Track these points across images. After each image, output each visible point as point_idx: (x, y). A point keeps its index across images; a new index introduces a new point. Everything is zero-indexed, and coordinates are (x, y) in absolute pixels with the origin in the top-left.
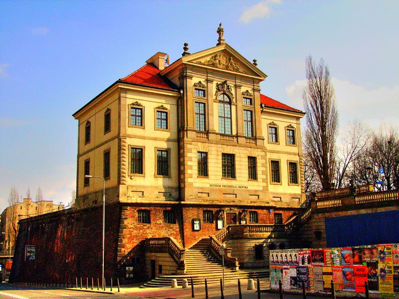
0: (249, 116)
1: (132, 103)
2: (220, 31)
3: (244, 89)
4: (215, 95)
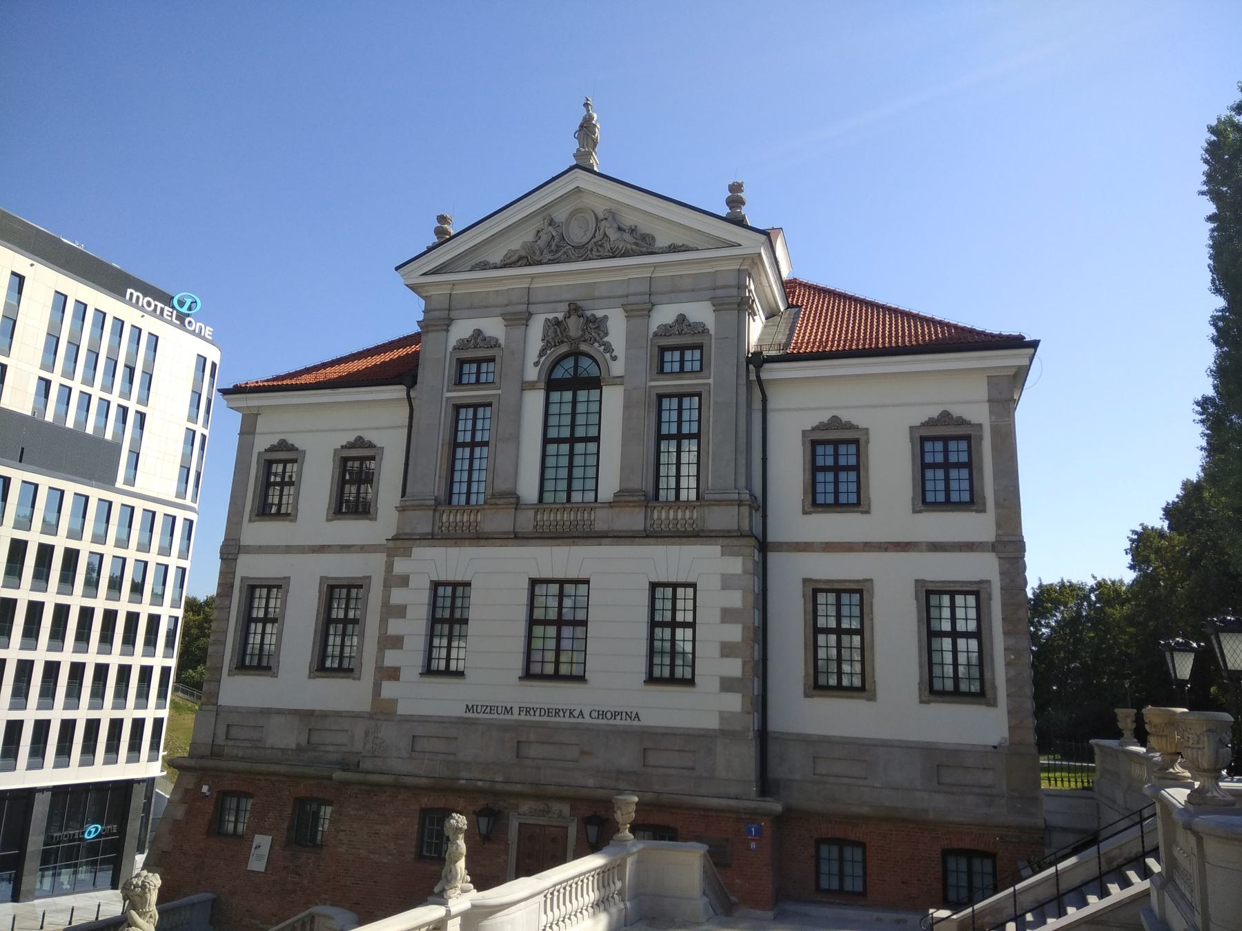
1: (268, 446)
2: (586, 129)
3: (664, 315)
4: (536, 364)
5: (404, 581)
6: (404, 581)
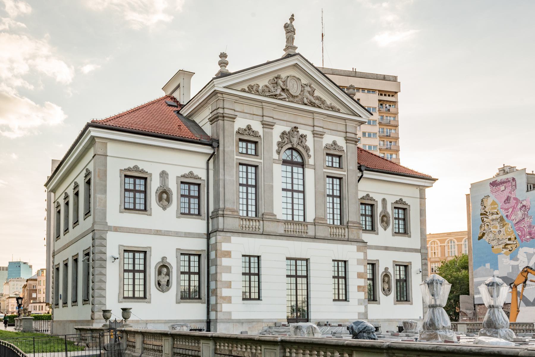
0: (337, 187)
3: (328, 139)
5: (228, 254)
6: (228, 254)
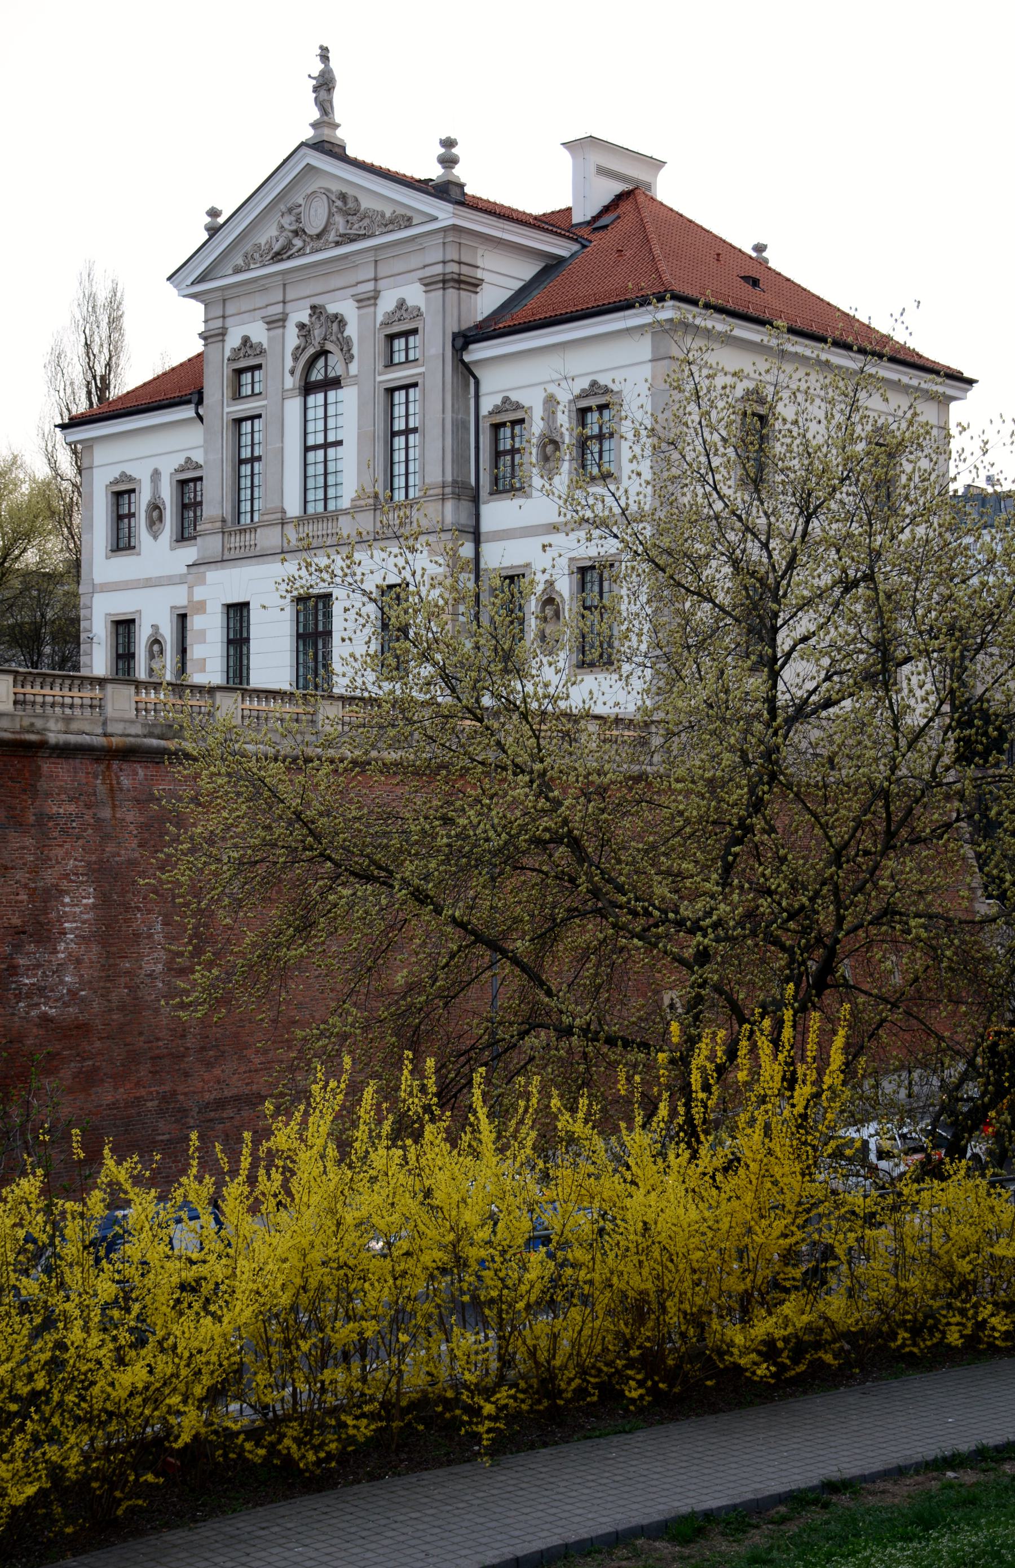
2: (324, 85)
3: (387, 304)
